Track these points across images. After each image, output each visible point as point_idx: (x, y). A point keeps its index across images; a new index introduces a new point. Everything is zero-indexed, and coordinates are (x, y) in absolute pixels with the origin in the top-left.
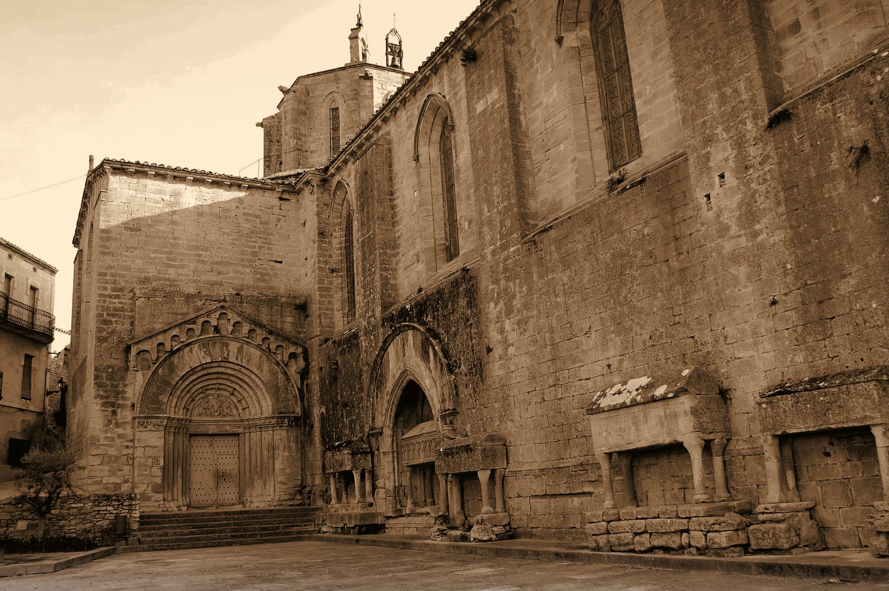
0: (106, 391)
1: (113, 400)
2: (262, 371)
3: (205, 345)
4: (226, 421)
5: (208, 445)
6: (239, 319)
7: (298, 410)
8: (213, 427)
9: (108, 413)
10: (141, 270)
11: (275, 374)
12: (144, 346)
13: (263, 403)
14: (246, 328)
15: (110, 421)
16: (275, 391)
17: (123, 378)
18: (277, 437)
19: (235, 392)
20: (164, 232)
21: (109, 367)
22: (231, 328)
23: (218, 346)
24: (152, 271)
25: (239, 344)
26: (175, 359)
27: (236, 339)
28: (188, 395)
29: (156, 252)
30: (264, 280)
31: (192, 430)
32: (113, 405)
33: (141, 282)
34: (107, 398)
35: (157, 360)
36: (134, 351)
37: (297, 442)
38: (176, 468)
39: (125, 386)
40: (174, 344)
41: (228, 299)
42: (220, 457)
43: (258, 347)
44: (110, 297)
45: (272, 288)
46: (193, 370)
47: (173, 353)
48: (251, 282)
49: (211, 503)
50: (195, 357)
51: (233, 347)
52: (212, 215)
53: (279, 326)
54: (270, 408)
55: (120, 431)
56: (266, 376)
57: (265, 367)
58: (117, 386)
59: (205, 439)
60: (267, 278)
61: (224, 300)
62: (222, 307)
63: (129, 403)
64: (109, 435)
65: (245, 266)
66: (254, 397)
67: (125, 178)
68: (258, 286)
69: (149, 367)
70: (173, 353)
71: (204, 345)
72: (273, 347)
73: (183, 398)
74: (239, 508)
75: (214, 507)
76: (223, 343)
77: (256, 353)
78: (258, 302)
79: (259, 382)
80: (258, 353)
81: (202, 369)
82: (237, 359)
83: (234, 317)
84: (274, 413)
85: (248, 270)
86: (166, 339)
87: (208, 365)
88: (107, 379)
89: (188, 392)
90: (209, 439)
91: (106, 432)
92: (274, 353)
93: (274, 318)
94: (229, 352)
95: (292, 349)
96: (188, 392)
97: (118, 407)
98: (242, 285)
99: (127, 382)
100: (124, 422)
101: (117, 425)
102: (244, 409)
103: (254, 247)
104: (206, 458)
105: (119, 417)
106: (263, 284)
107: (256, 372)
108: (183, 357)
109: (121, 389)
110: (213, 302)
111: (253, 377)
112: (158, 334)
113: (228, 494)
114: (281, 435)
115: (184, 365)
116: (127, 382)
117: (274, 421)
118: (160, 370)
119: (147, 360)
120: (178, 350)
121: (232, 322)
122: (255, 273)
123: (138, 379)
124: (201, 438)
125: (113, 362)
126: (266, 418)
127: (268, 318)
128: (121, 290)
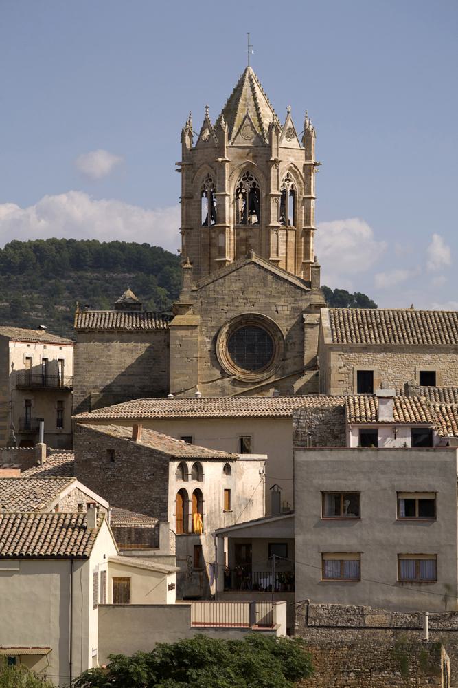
10: (93, 382)
20: (104, 361)
24: (99, 382)
29: (101, 372)
33: (94, 388)
44: (79, 396)
52: (128, 349)
65: (145, 375)
67: (84, 335)
85: (147, 378)
103: (150, 365)
128: (85, 392)
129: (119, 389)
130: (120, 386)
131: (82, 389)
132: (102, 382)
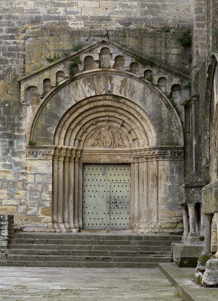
0: (4, 124)
1: (10, 132)
2: (145, 103)
3: (90, 78)
4: (117, 152)
5: (101, 173)
6: (121, 53)
7: (181, 141)
8: (105, 157)
9: (5, 143)
11: (159, 106)
12: (32, 82)
13: (149, 135)
14: (128, 62)
15: (8, 151)
16: (159, 124)
17: (19, 112)
18: (160, 167)
19: (125, 124)
21: (6, 102)
22: (112, 62)
23: (102, 79)
25: (122, 78)
26: (62, 94)
27: (119, 73)
28: (79, 127)
30: (151, 12)
31: (85, 159)
32: (10, 136)
34: (5, 130)
35: (44, 95)
36: (23, 88)
37: (180, 173)
38: (68, 197)
39: (21, 119)
40: (60, 79)
41: (110, 33)
42: (113, 185)
43: (141, 79)
45: (160, 19)
46: (79, 104)
47: (59, 88)
48: (139, 15)
49: (104, 226)
50: (82, 91)
51: (117, 80)
53: (163, 58)
54: (155, 139)
55: (17, 159)
56: (150, 108)
57: (149, 99)
58: (13, 119)
59: (99, 168)
60: (155, 10)
61: (107, 35)
62: (103, 42)
63: (24, 134)
64: (7, 162)
66: (141, 128)
68: (145, 19)
69: (38, 101)
70: (59, 88)
71: (88, 79)
72: (156, 79)
73: (73, 130)
74: (128, 232)
75: (105, 231)
76: (107, 77)
77: (139, 86)
78: (141, 34)
79: (144, 115)
80: (142, 86)
81: (89, 103)
82: (121, 92)
83: (115, 52)
84: (158, 144)
86: (51, 75)
87: (93, 99)
88: (5, 113)
89: (78, 124)
90: (103, 168)
91: (4, 160)
92: (158, 86)
93: (158, 51)
94: (112, 85)
95: (176, 81)
96: (78, 124)
97: (15, 138)
98: (129, 19)
99: (22, 115)
100: (20, 152)
101: (14, 154)
102: (134, 140)
104: (99, 186)
105: (15, 147)
106: (151, 17)
107: (139, 103)
108: (69, 92)
109: (17, 122)
110: (96, 38)
111: (138, 109)
112: (43, 71)
113: (121, 219)
114: (165, 165)
115: (70, 99)
116: (22, 115)
117: (157, 152)
118: (48, 105)
119: (37, 95)
120: (64, 85)
121: (114, 56)
122: (143, 6)
123: (28, 113)
124: (95, 167)
125: (8, 97)
126: (151, 149)
127: (152, 50)
129: (80, 25)
130: (84, 18)
131: (9, 24)
132: (49, 12)
